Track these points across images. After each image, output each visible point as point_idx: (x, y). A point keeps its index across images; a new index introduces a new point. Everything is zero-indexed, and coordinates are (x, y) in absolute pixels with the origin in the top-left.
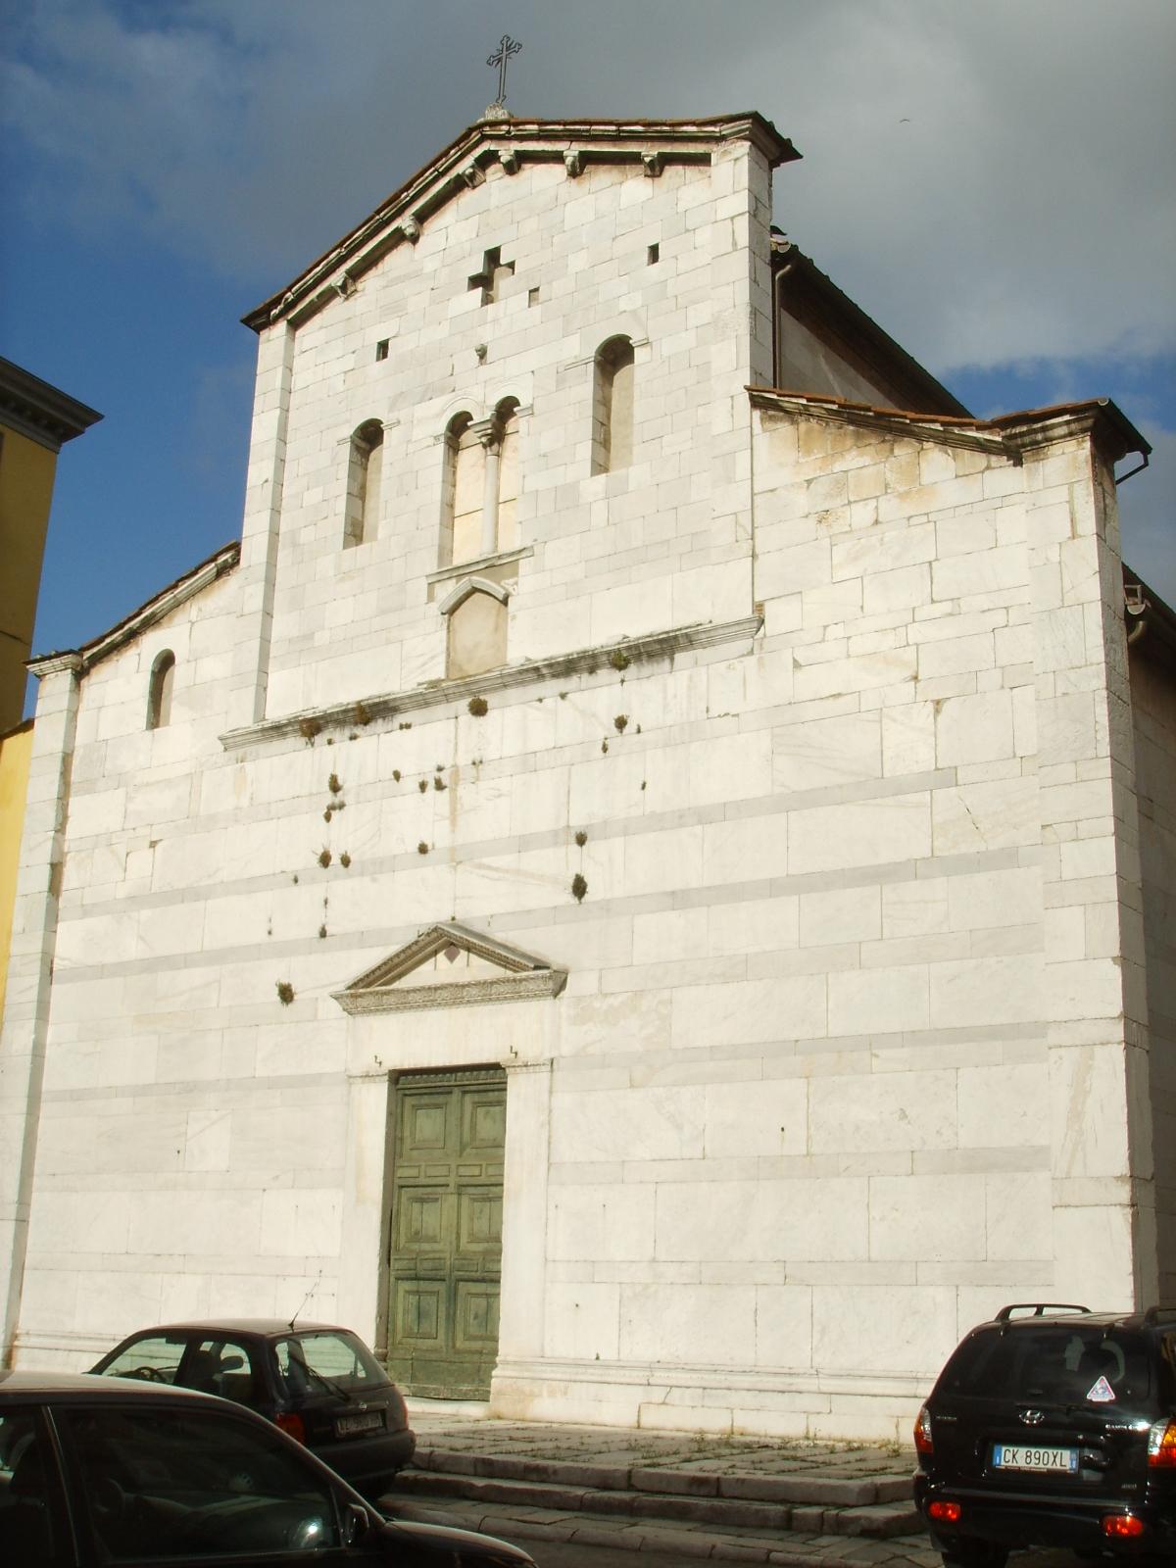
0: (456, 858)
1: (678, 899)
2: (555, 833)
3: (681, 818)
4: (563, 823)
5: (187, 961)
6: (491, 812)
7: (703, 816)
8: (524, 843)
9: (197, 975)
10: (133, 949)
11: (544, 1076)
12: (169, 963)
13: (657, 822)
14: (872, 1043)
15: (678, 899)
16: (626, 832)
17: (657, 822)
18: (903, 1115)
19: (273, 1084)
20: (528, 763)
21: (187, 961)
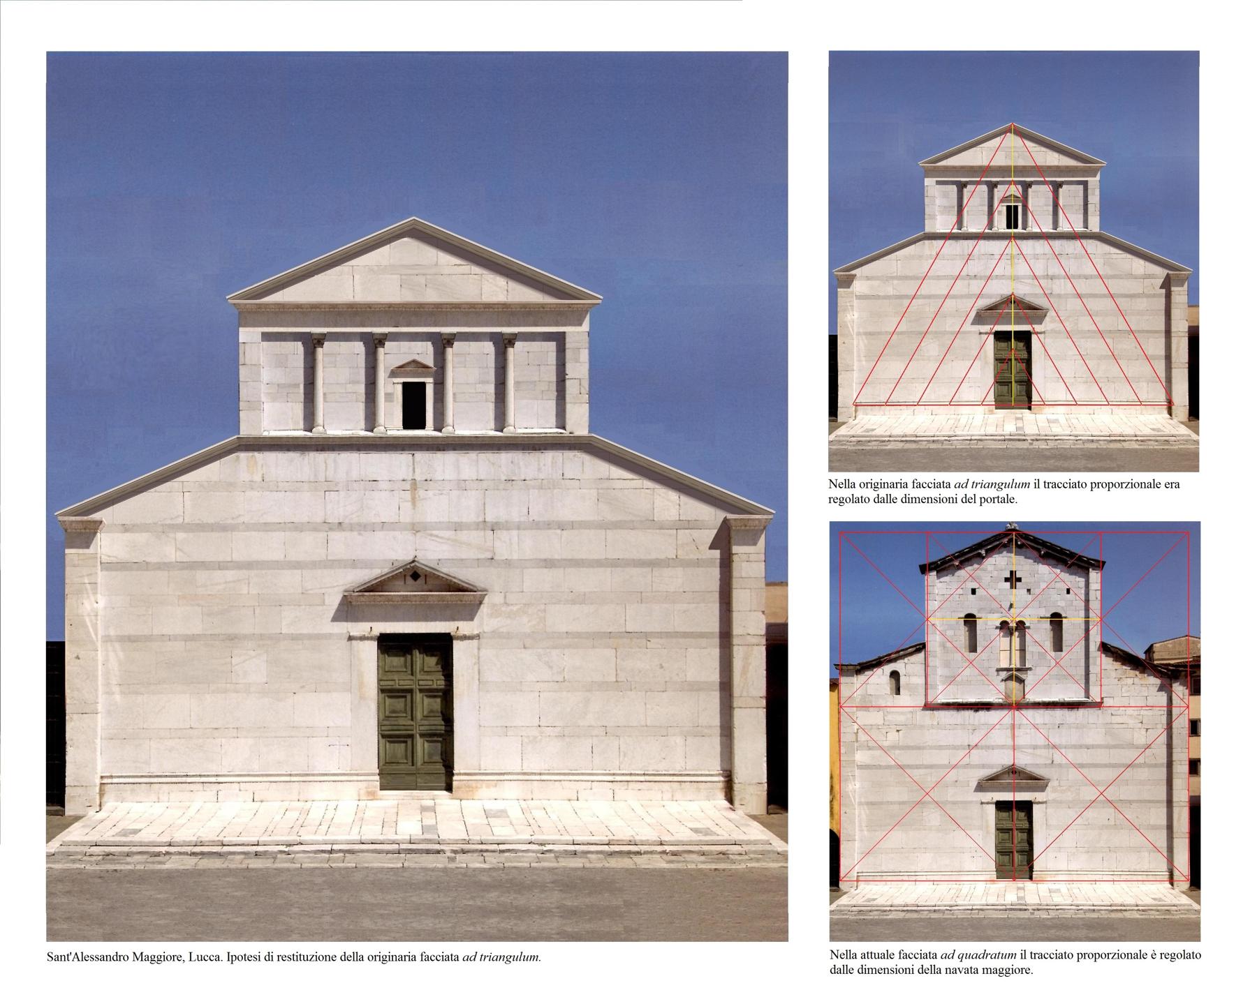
0: (416, 528)
1: (549, 564)
2: (478, 524)
3: (548, 525)
4: (481, 519)
5: (221, 566)
6: (435, 508)
7: (562, 526)
8: (458, 527)
9: (230, 575)
10: (171, 555)
11: (475, 642)
12: (204, 565)
13: (536, 526)
14: (647, 636)
15: (549, 564)
16: (519, 528)
17: (536, 526)
18: (662, 667)
19: (295, 638)
20: (462, 485)
21: (221, 566)
